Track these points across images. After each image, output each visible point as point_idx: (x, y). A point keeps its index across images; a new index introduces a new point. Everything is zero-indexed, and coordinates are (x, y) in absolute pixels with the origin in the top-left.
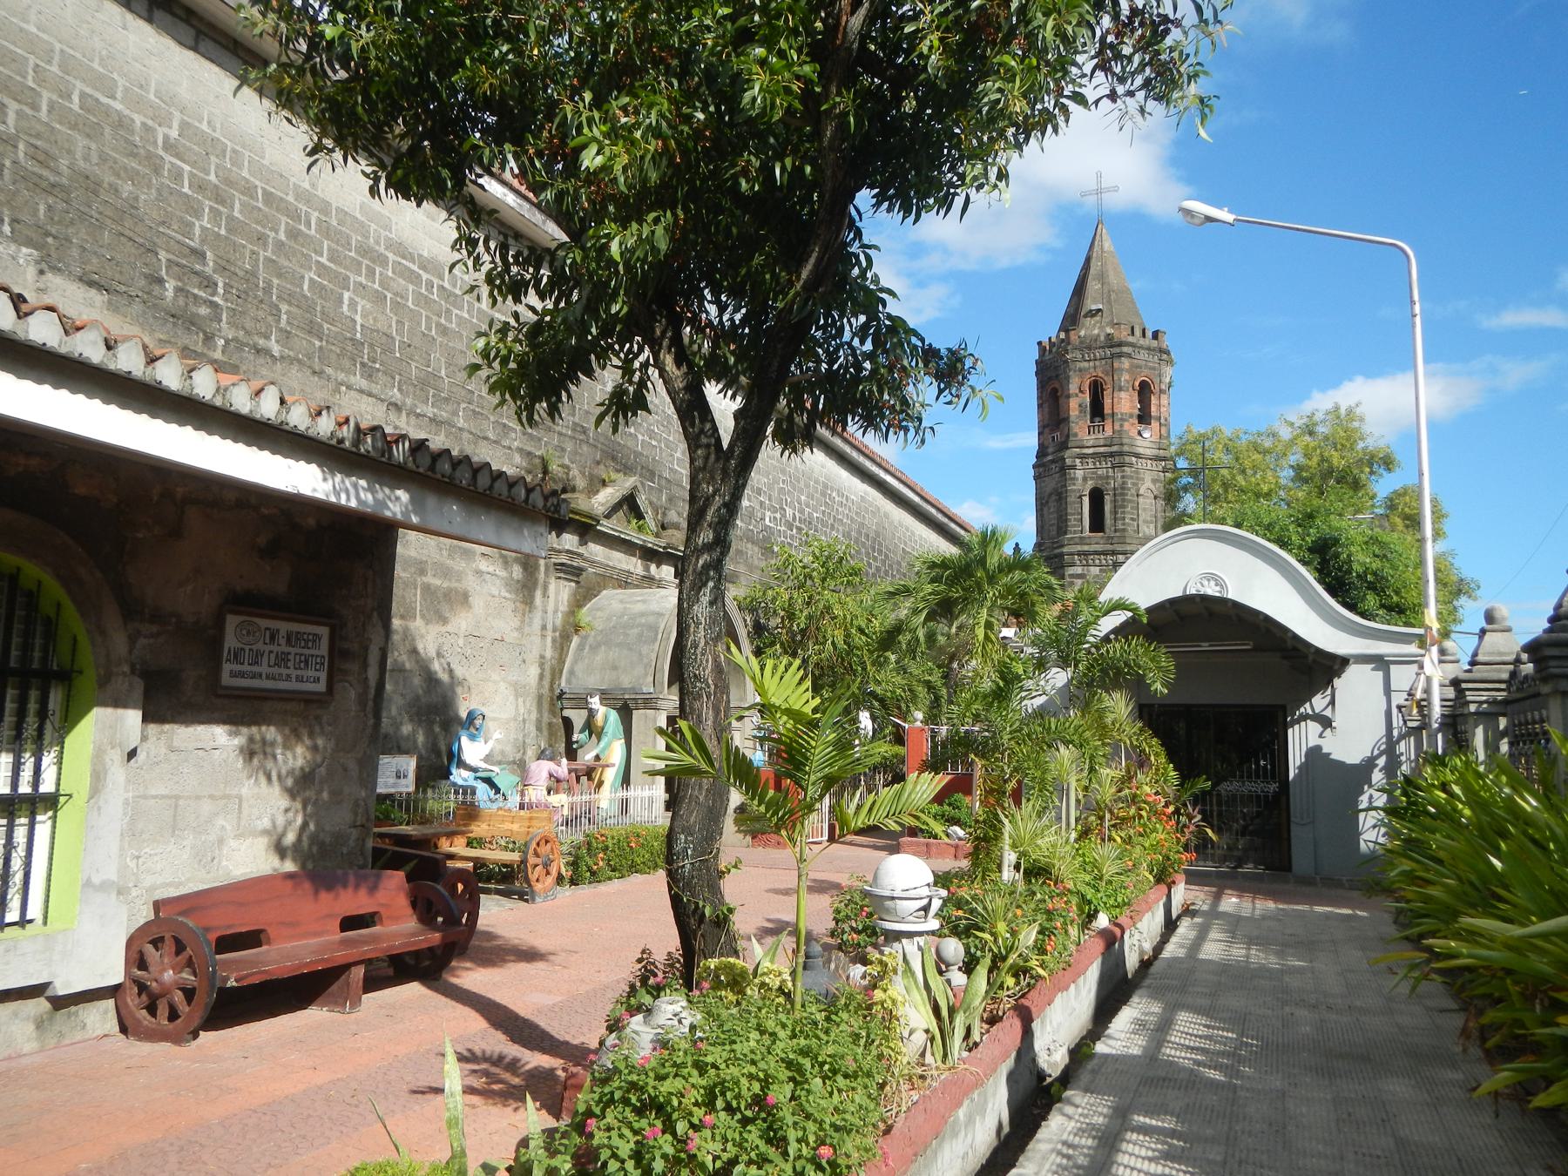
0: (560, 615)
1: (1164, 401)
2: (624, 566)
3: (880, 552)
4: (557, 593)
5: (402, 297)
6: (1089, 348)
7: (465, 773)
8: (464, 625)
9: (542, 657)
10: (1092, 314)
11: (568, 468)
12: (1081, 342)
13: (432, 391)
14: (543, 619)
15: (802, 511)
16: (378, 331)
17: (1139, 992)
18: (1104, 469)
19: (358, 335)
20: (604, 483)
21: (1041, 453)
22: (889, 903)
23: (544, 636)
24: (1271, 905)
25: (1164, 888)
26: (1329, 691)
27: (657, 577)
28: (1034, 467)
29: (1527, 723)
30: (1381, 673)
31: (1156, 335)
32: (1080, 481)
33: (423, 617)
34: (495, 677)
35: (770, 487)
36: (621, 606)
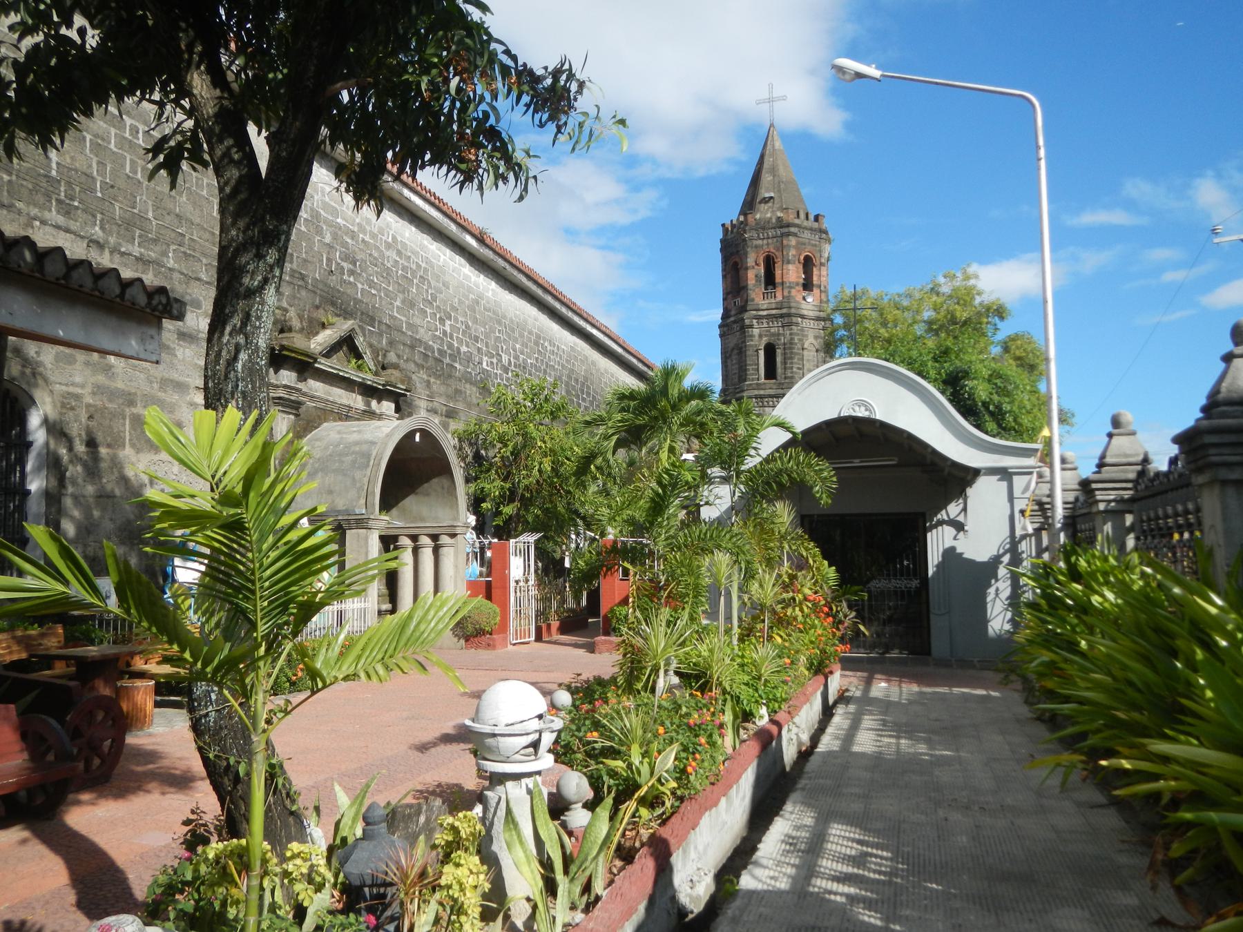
1: (824, 272)
2: (345, 402)
3: (588, 394)
5: (103, 139)
6: (764, 228)
10: (766, 201)
11: (286, 310)
12: (757, 224)
13: (138, 232)
15: (517, 358)
16: (76, 170)
17: (794, 796)
18: (775, 327)
19: (54, 173)
20: (323, 326)
21: (725, 316)
22: (490, 741)
24: (915, 688)
25: (821, 678)
26: (961, 501)
27: (378, 411)
28: (720, 327)
29: (1158, 518)
30: (1005, 484)
31: (817, 218)
32: (757, 338)
33: (133, 445)
35: (487, 335)
36: (338, 436)
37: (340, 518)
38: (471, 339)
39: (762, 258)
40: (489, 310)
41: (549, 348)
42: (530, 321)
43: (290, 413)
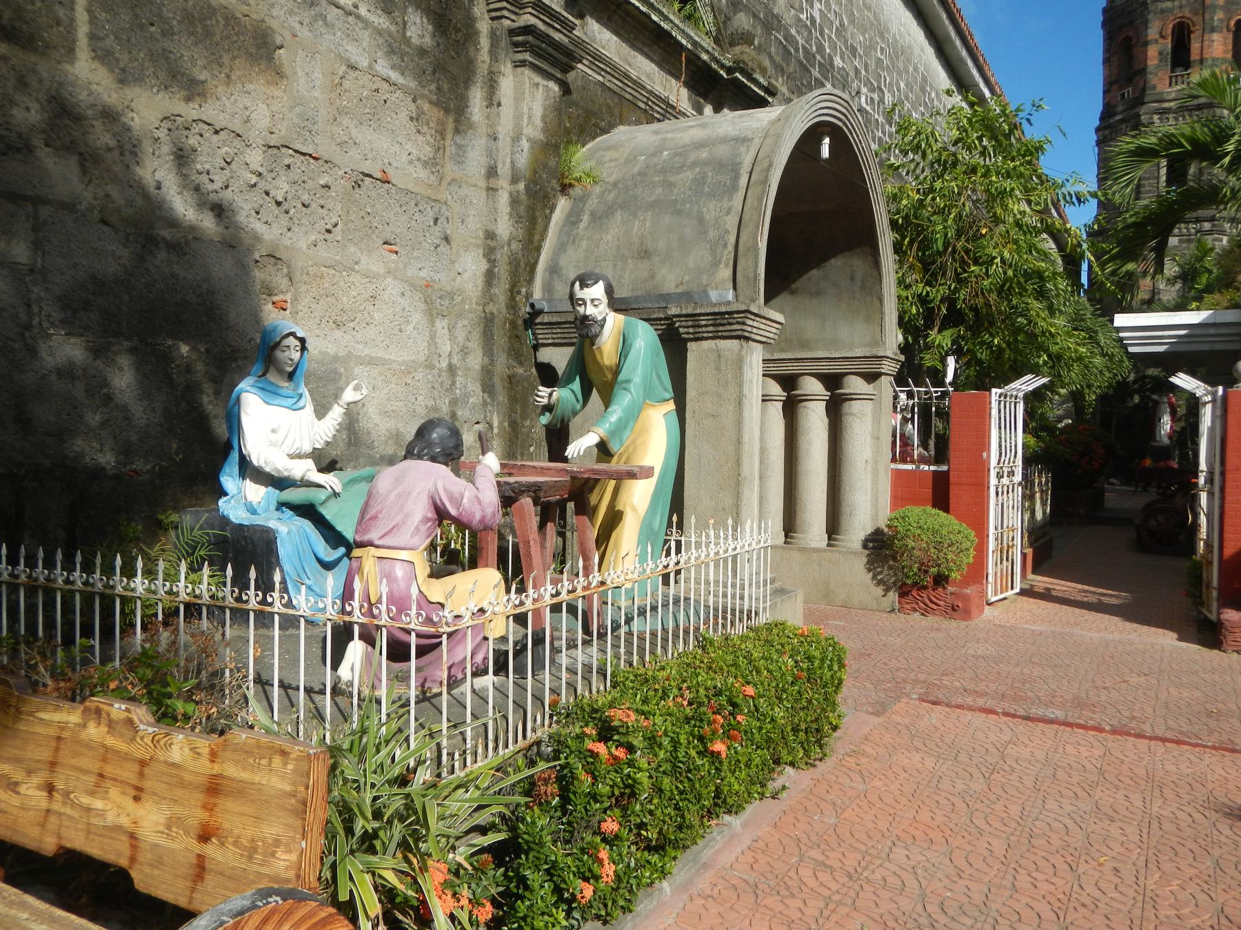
0: (525, 145)
2: (658, 89)
4: (518, 98)
7: (256, 493)
8: (261, 117)
9: (490, 235)
14: (490, 153)
23: (491, 190)
33: (102, 56)
34: (375, 261)
37: (673, 311)
38: (847, 48)
39: (1171, 26)
40: (869, 9)
41: (936, 103)
42: (917, 51)
43: (548, 76)
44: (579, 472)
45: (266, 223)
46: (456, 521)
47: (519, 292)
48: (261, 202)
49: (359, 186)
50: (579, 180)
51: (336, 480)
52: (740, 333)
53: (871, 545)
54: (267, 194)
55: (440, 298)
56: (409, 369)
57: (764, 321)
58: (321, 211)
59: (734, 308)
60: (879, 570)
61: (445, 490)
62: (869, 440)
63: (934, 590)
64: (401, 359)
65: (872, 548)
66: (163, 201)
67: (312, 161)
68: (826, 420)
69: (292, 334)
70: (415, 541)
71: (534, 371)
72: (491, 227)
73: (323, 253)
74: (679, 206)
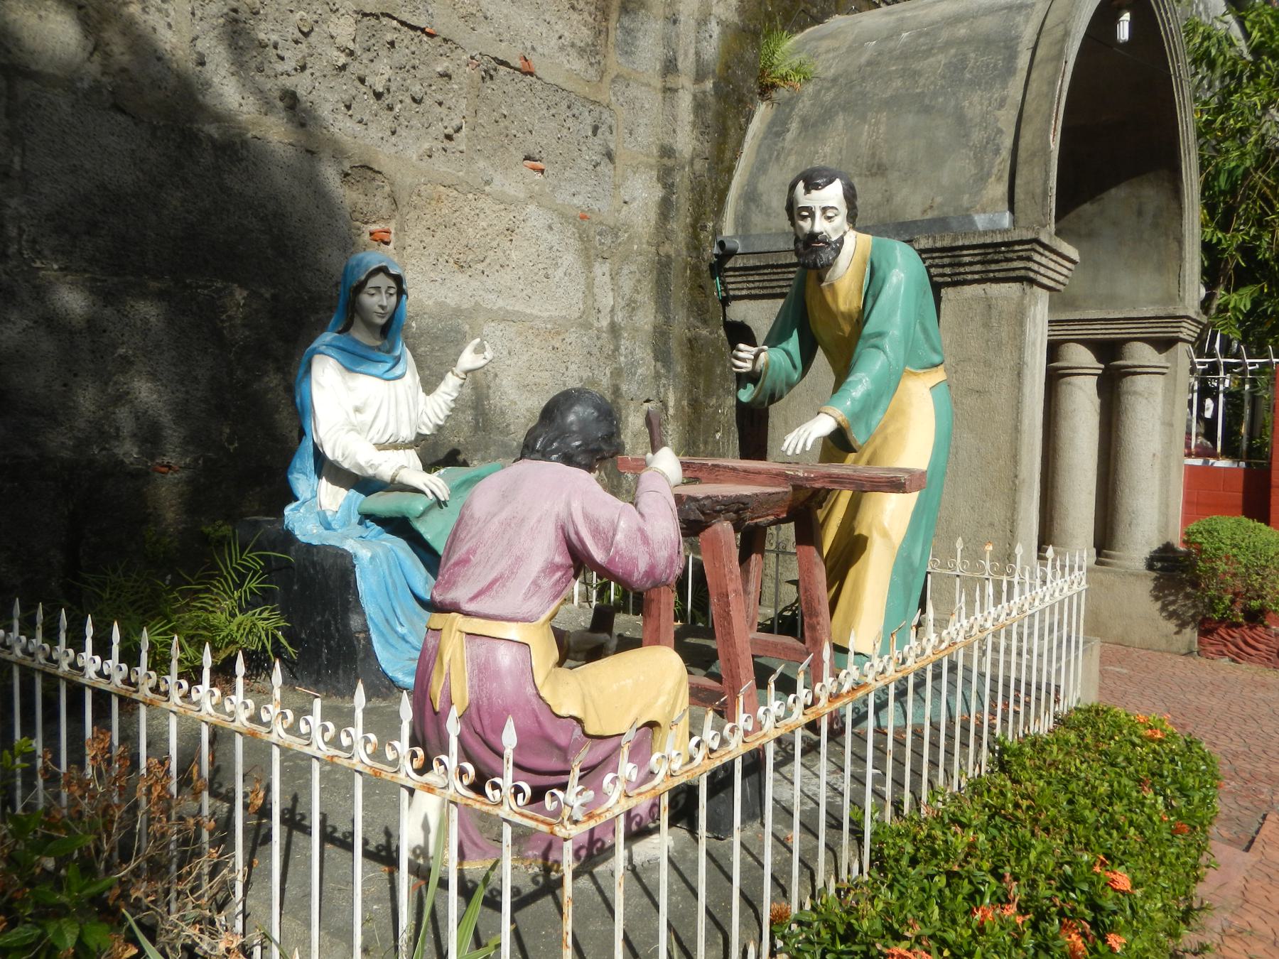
0: (715, 29)
7: (332, 497)
14: (667, 42)
23: (669, 91)
44: (807, 479)
45: (360, 122)
46: (603, 572)
47: (704, 228)
48: (354, 92)
49: (491, 77)
50: (784, 78)
51: (440, 482)
52: (1023, 273)
53: (1159, 565)
54: (362, 81)
55: (600, 234)
56: (558, 328)
57: (1055, 257)
58: (438, 109)
59: (1015, 236)
60: (1171, 598)
61: (586, 516)
62: (1158, 427)
63: (1251, 629)
64: (546, 314)
65: (1160, 569)
66: (208, 84)
67: (425, 38)
68: (1097, 401)
69: (383, 270)
70: (533, 605)
71: (722, 332)
72: (667, 140)
73: (440, 166)
74: (927, 101)
